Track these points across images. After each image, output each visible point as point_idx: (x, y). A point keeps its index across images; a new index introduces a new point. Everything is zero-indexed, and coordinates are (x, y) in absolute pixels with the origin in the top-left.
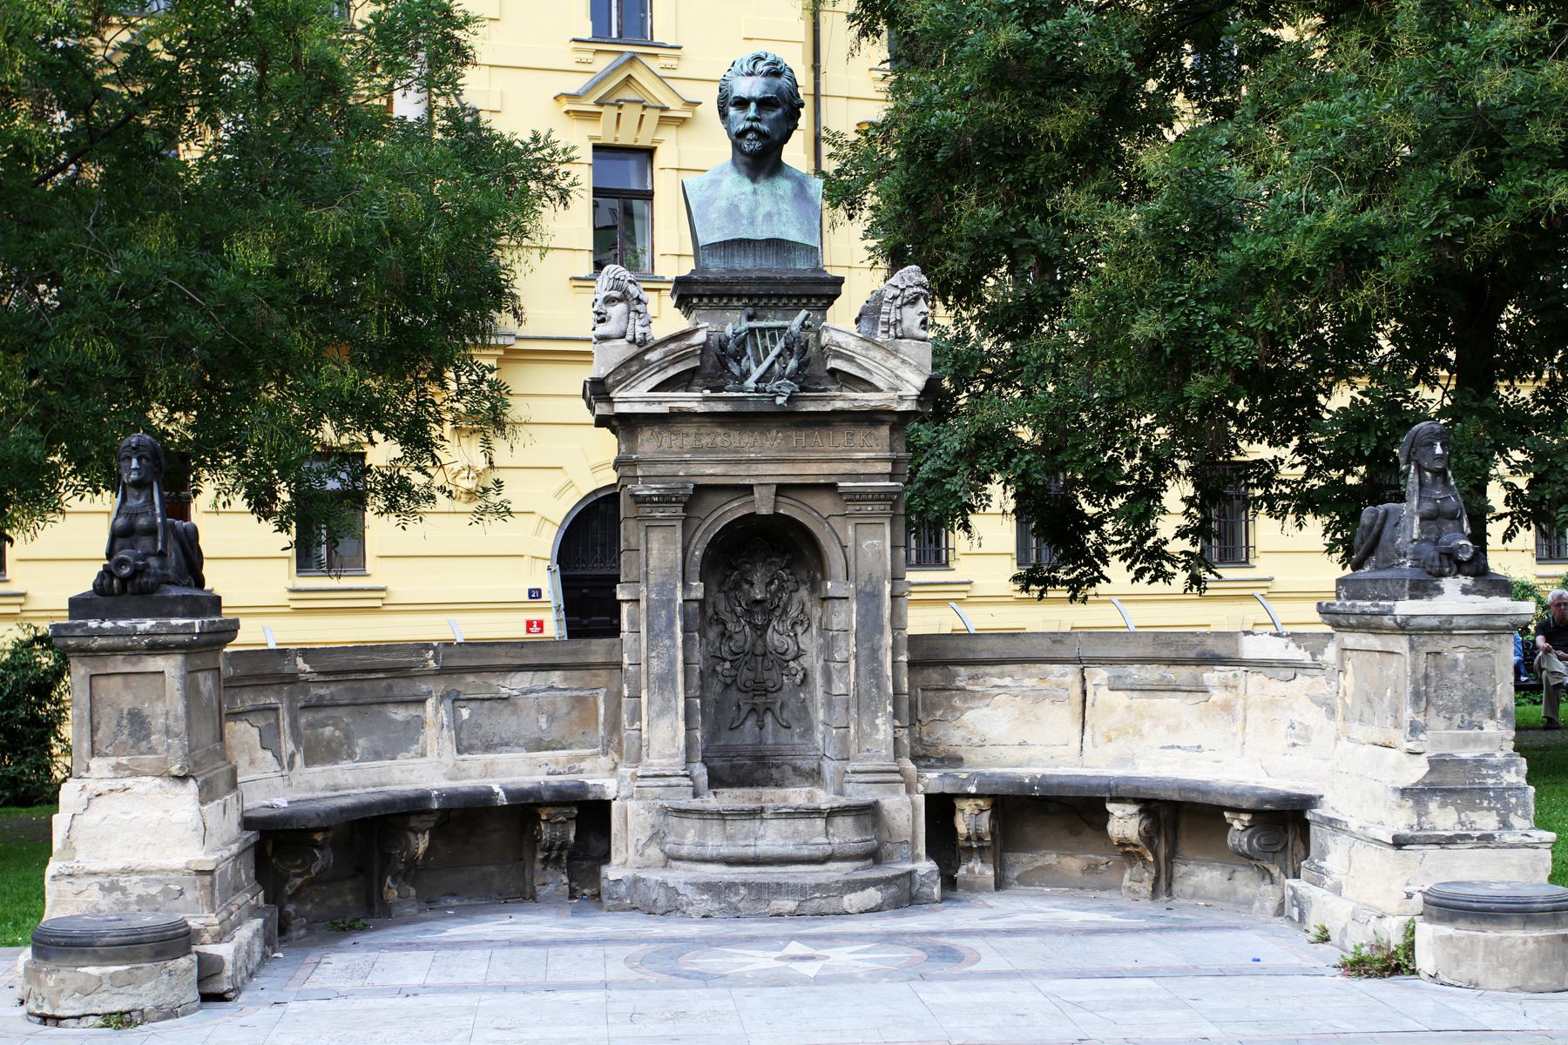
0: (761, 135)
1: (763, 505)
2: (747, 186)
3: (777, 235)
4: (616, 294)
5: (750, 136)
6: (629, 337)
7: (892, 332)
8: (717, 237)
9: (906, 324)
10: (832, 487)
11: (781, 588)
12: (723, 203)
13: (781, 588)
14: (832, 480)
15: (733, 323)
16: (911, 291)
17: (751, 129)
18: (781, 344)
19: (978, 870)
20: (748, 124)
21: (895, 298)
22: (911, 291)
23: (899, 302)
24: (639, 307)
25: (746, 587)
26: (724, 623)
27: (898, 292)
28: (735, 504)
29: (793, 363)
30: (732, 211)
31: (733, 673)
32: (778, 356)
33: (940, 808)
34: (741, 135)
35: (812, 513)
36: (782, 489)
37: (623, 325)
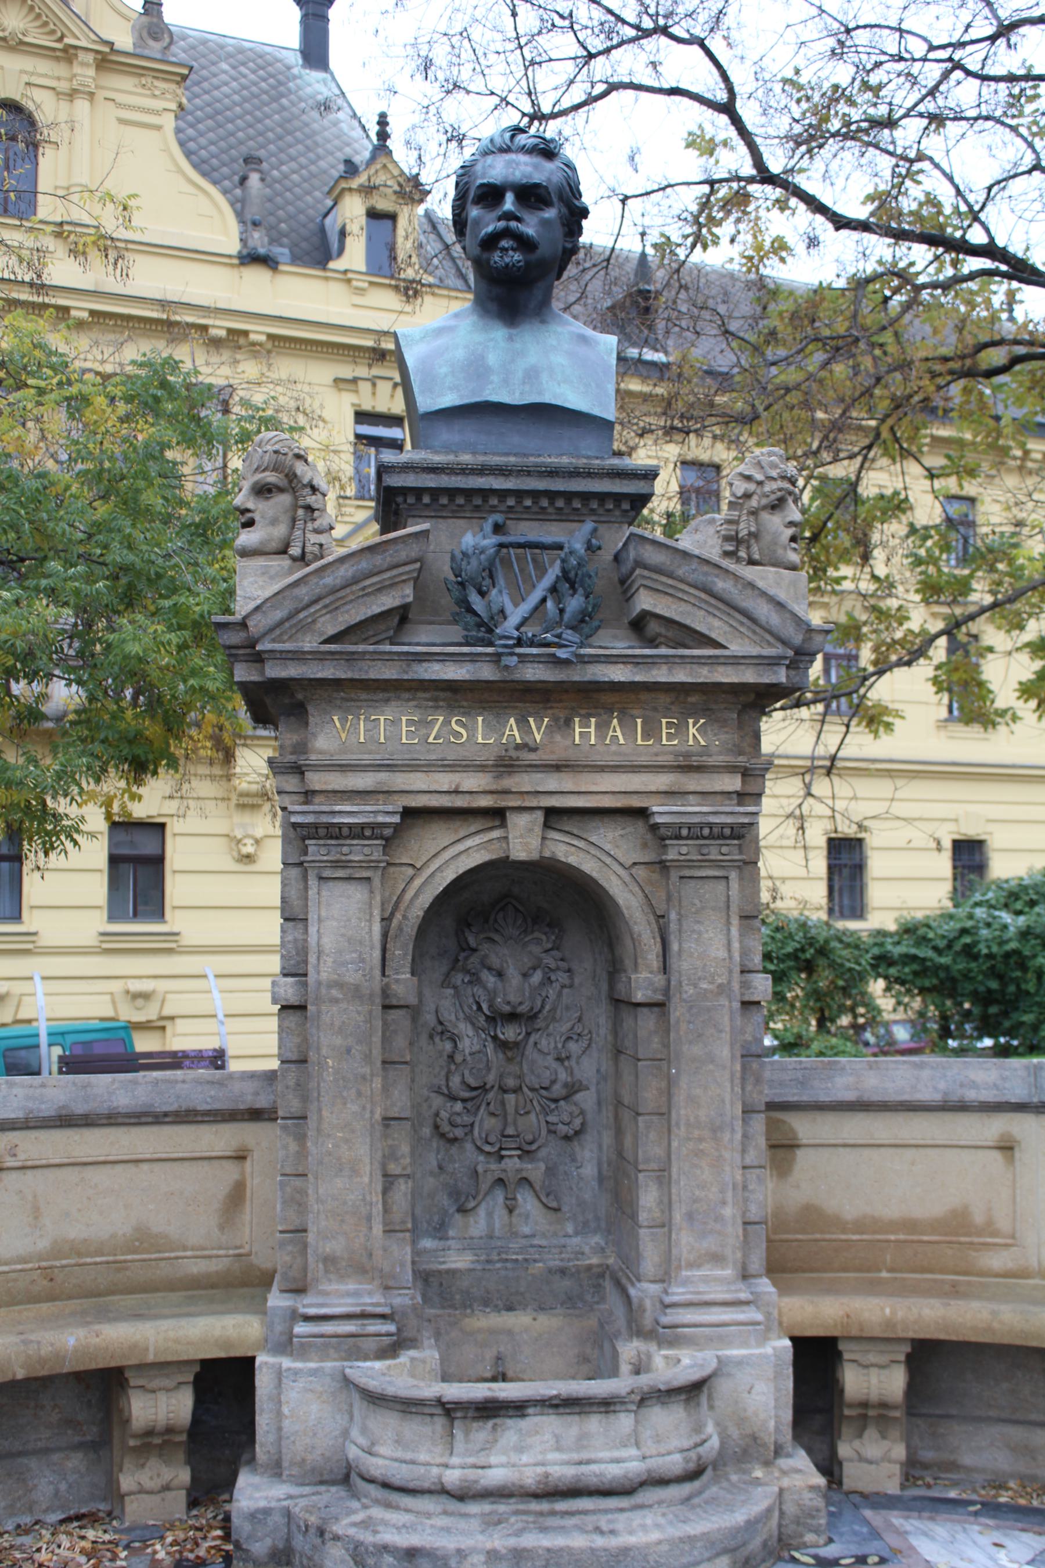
0: (525, 243)
1: (523, 840)
2: (499, 333)
3: (547, 399)
4: (271, 477)
5: (504, 243)
6: (295, 551)
7: (742, 554)
8: (448, 400)
9: (766, 539)
10: (642, 813)
11: (547, 981)
12: (460, 354)
13: (547, 981)
14: (636, 802)
15: (473, 538)
16: (774, 485)
17: (506, 233)
18: (553, 572)
19: (874, 1459)
20: (502, 224)
21: (747, 496)
22: (774, 485)
23: (754, 503)
24: (311, 500)
25: (490, 980)
26: (454, 1039)
27: (752, 487)
28: (469, 843)
29: (574, 604)
30: (476, 368)
31: (467, 1119)
32: (553, 590)
33: (816, 1360)
34: (490, 242)
35: (605, 859)
36: (553, 816)
37: (280, 531)
